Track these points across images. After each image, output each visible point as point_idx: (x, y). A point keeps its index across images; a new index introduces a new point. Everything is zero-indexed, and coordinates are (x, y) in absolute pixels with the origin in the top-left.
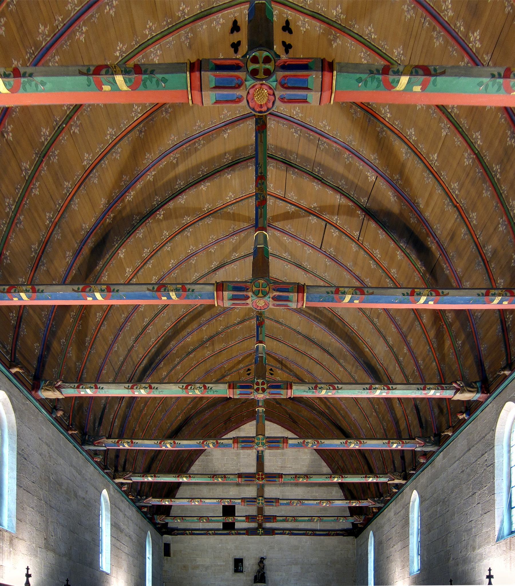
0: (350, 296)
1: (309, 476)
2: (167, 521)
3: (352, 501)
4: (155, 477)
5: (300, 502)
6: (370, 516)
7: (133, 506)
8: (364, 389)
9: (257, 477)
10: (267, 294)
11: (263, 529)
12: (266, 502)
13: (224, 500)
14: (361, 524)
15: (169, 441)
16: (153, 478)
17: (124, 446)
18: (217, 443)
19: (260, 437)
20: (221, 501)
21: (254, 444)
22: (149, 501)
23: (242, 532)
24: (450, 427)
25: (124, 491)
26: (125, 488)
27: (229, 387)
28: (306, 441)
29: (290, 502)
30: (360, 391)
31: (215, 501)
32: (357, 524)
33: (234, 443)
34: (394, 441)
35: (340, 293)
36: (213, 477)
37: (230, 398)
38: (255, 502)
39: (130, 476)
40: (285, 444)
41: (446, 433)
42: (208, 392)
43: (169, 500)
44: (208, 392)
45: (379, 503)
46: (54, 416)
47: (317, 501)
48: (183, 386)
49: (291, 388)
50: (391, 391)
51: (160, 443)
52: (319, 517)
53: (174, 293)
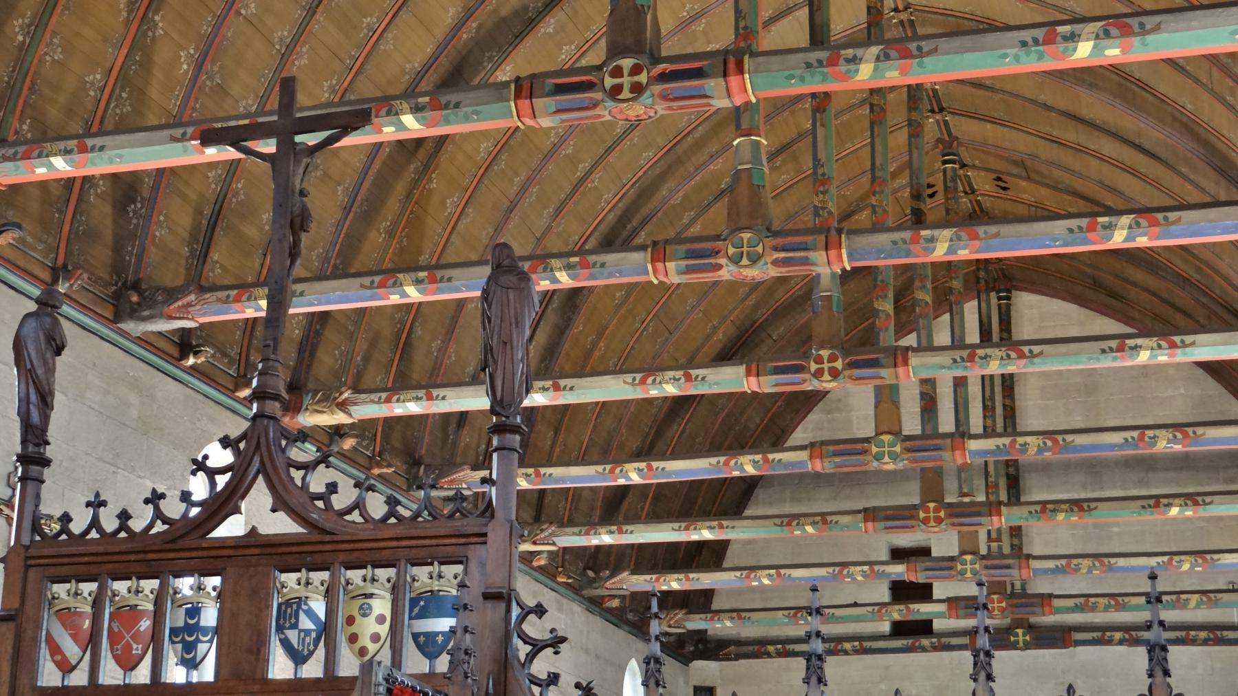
0: (946, 245)
1: (1085, 505)
4: (620, 532)
5: (1103, 564)
7: (574, 600)
8: (1104, 351)
9: (922, 515)
10: (760, 257)
11: (1031, 628)
12: (987, 567)
13: (852, 569)
15: (636, 465)
16: (616, 536)
18: (766, 460)
19: (886, 438)
20: (841, 572)
22: (621, 581)
23: (955, 641)
25: (541, 569)
27: (748, 373)
29: (1068, 565)
33: (811, 457)
35: (922, 241)
36: (789, 524)
38: (951, 568)
40: (958, 453)
43: (681, 576)
48: (634, 379)
49: (906, 363)
50: (1179, 351)
51: (612, 471)
53: (564, 273)
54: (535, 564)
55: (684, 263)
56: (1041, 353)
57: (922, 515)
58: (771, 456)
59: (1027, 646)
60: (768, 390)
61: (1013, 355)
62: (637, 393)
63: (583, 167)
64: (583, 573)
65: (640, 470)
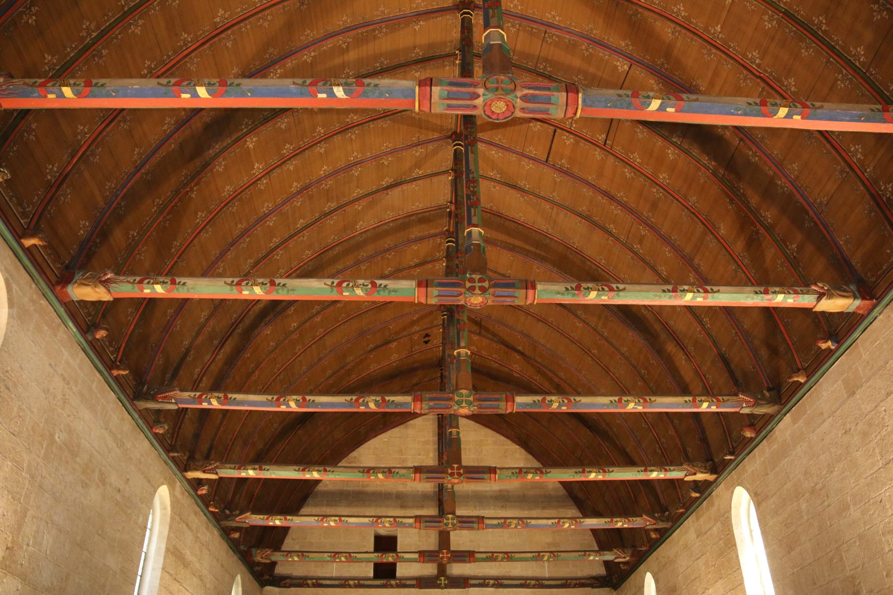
2: (274, 558)
3: (615, 520)
4: (261, 469)
5: (523, 522)
6: (643, 549)
7: (215, 527)
8: (664, 291)
11: (448, 578)
12: (460, 522)
13: (383, 519)
14: (625, 563)
15: (295, 397)
16: (258, 471)
17: (210, 403)
18: (384, 400)
20: (377, 521)
21: (453, 403)
22: (246, 518)
24: (799, 370)
25: (201, 497)
26: (204, 491)
27: (419, 285)
28: (548, 398)
29: (505, 522)
30: (658, 294)
31: (366, 520)
32: (619, 563)
33: (414, 401)
34: (703, 398)
36: (368, 472)
37: (420, 303)
38: (440, 522)
39: (217, 467)
40: (510, 404)
41: (796, 379)
42: (378, 292)
43: (282, 518)
44: (378, 292)
45: (663, 521)
46: (90, 338)
47: (553, 521)
48: (333, 283)
50: (710, 295)
52: (551, 552)
54: (199, 492)
55: (449, 88)
56: (624, 289)
57: (450, 471)
58: (387, 398)
59: (446, 587)
60: (433, 301)
61: (606, 289)
62: (334, 295)
63: (276, 240)
64: (223, 511)
65: (297, 401)
